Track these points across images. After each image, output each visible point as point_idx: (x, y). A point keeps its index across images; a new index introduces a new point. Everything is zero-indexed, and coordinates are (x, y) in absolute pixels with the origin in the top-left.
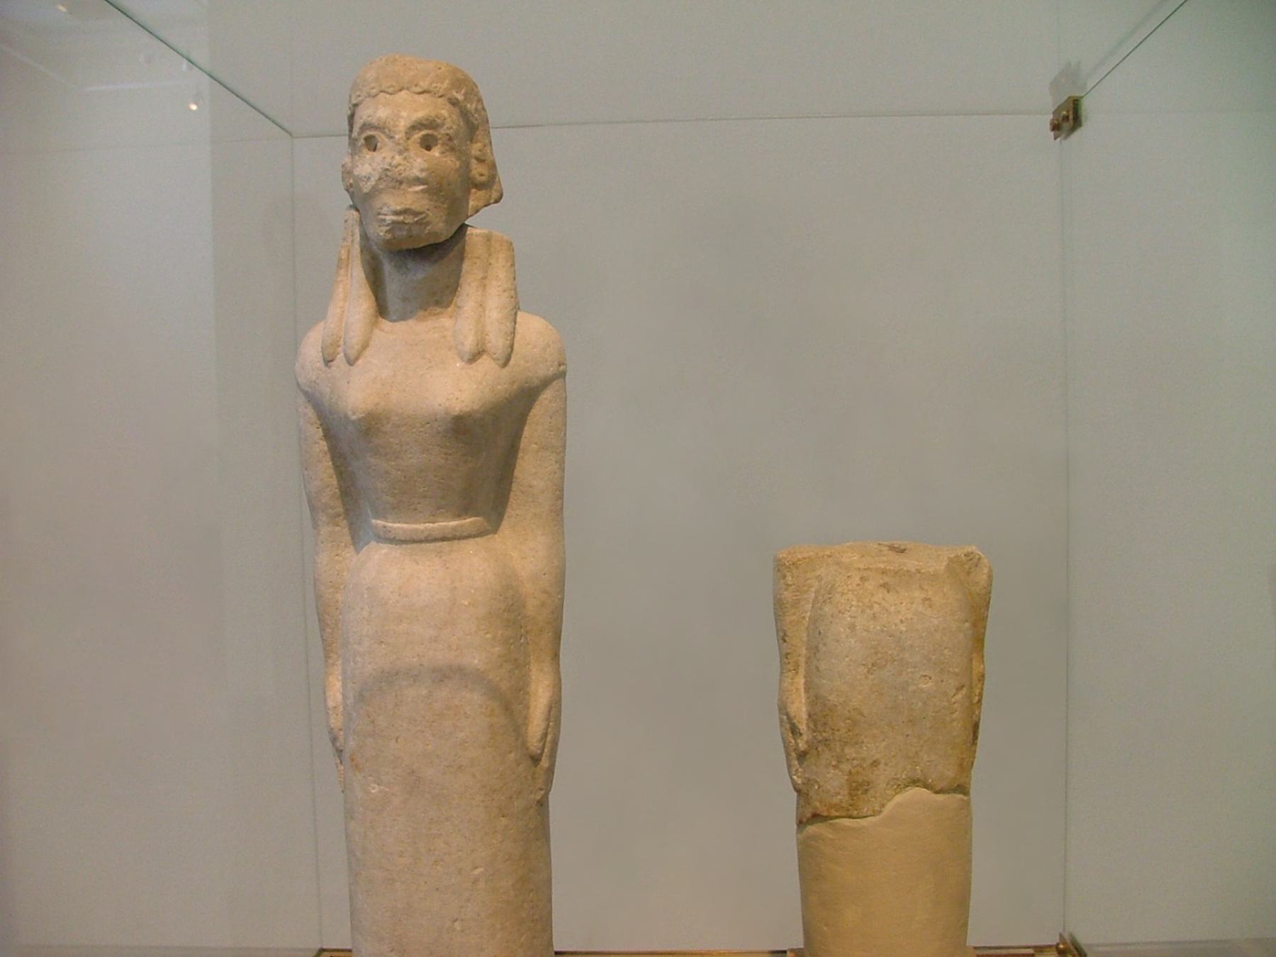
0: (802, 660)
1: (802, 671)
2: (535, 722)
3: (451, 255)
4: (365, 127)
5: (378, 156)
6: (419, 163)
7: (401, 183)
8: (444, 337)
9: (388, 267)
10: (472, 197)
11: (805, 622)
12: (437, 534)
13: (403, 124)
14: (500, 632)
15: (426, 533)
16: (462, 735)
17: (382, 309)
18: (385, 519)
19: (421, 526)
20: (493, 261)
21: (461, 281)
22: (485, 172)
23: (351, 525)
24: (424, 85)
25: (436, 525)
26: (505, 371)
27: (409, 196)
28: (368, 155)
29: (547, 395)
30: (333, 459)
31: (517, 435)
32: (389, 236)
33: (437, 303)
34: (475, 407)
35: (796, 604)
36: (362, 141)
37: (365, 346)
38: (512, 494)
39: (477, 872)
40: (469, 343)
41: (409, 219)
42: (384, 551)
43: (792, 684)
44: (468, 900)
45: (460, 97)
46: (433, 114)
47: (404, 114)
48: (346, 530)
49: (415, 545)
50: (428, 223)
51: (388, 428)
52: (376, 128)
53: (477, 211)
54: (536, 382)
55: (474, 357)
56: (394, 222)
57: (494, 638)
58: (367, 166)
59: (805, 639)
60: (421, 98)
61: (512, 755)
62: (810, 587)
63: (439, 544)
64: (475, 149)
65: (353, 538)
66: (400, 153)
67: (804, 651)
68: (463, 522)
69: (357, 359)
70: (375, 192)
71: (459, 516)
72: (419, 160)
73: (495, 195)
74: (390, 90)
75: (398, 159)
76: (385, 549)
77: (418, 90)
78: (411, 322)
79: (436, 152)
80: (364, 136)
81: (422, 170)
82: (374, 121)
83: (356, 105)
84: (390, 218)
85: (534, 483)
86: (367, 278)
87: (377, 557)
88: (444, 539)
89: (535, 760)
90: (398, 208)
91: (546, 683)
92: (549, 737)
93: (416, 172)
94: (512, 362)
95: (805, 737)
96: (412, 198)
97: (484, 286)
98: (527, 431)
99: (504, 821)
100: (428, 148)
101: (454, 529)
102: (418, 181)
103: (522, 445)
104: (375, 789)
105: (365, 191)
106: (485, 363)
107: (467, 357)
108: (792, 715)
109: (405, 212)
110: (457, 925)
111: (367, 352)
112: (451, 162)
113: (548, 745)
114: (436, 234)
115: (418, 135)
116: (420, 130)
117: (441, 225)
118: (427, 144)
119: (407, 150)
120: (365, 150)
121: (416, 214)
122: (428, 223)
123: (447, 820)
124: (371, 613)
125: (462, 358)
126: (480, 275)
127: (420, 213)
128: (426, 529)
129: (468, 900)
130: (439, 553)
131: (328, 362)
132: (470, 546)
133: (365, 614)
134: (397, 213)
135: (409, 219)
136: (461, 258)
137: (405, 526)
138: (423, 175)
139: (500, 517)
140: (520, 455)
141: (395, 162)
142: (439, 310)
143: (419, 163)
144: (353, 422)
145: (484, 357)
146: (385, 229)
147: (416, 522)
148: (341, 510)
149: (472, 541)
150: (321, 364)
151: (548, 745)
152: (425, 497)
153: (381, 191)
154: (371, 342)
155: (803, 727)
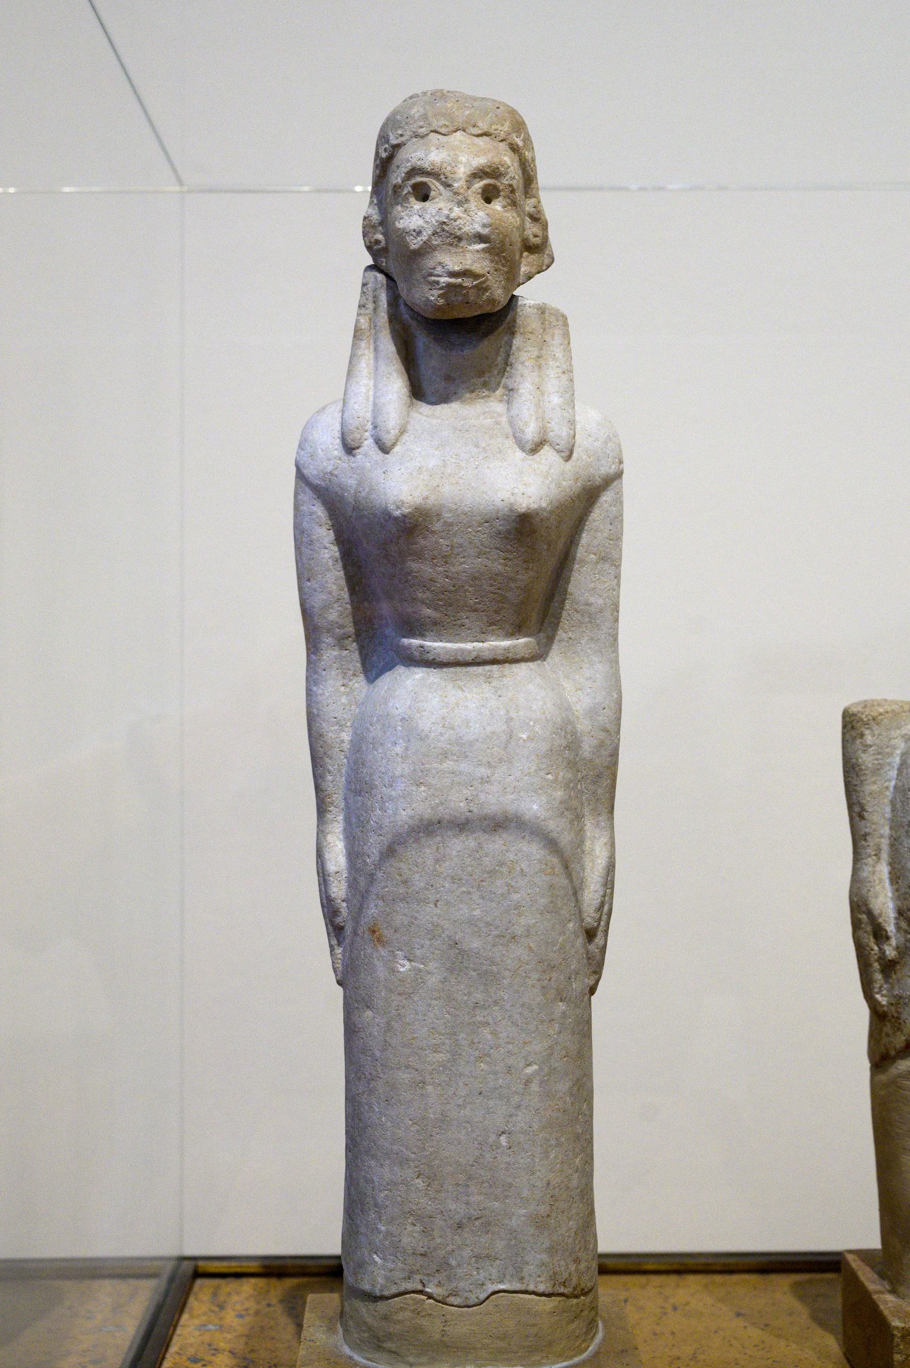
0: (885, 843)
1: (885, 856)
2: (592, 887)
3: (501, 329)
4: (414, 171)
5: (430, 207)
6: (477, 217)
7: (460, 239)
8: (498, 423)
9: (422, 340)
10: (524, 261)
11: (889, 794)
12: (487, 655)
13: (462, 172)
14: (561, 774)
15: (474, 654)
16: (515, 897)
17: (417, 392)
18: (422, 636)
19: (469, 646)
20: (548, 338)
21: (512, 359)
22: (540, 233)
23: (361, 649)
24: (483, 126)
25: (486, 645)
26: (569, 466)
27: (468, 256)
28: (417, 205)
29: (606, 498)
30: (345, 567)
31: (573, 540)
32: (441, 302)
33: (485, 385)
34: (544, 505)
35: (878, 770)
36: (408, 189)
37: (403, 431)
38: (564, 613)
39: (529, 1070)
40: (531, 432)
41: (468, 282)
42: (417, 676)
43: (874, 873)
44: (518, 1107)
45: (521, 144)
46: (496, 160)
47: (463, 159)
48: (356, 656)
49: (459, 669)
50: (486, 289)
51: (437, 526)
52: (434, 174)
53: (530, 278)
54: (598, 481)
55: (535, 449)
56: (449, 286)
57: (555, 781)
58: (416, 218)
59: (888, 816)
60: (482, 142)
61: (571, 925)
62: (895, 748)
63: (488, 668)
64: (529, 206)
65: (364, 664)
66: (460, 204)
67: (886, 831)
68: (516, 642)
69: (394, 445)
70: (426, 249)
71: (510, 635)
72: (481, 213)
73: (546, 261)
74: (443, 130)
75: (457, 211)
76: (419, 674)
77: (477, 131)
78: (455, 406)
79: (497, 206)
80: (413, 181)
81: (484, 226)
82: (427, 165)
83: (398, 146)
84: (444, 280)
85: (592, 600)
86: (399, 352)
87: (409, 682)
88: (494, 662)
89: (590, 934)
90: (457, 268)
91: (605, 840)
92: (606, 908)
93: (478, 228)
94: (575, 455)
95: (893, 942)
96: (471, 257)
97: (540, 367)
98: (585, 539)
99: (562, 1006)
100: (488, 200)
101: (507, 649)
102: (481, 238)
103: (578, 555)
104: (404, 967)
105: (413, 247)
106: (547, 455)
107: (528, 447)
108: (876, 912)
109: (465, 273)
110: (503, 1140)
111: (405, 437)
112: (511, 218)
113: (604, 917)
114: (492, 301)
115: (479, 185)
116: (481, 178)
117: (500, 291)
118: (488, 196)
119: (467, 201)
120: (412, 200)
121: (476, 276)
122: (486, 289)
123: (496, 1003)
124: (407, 749)
125: (522, 448)
126: (536, 353)
127: (483, 276)
128: (474, 649)
129: (518, 1107)
130: (489, 678)
131: (350, 449)
132: (522, 670)
133: (398, 749)
134: (453, 274)
135: (468, 282)
136: (512, 333)
137: (449, 645)
138: (485, 231)
139: (550, 640)
140: (576, 566)
141: (453, 215)
142: (487, 393)
143: (477, 217)
144: (396, 519)
145: (545, 447)
146: (436, 293)
147: (461, 641)
148: (351, 630)
149: (523, 666)
150: (337, 450)
151: (604, 917)
152: (475, 611)
153: (434, 248)
154: (409, 427)
155: (891, 928)
